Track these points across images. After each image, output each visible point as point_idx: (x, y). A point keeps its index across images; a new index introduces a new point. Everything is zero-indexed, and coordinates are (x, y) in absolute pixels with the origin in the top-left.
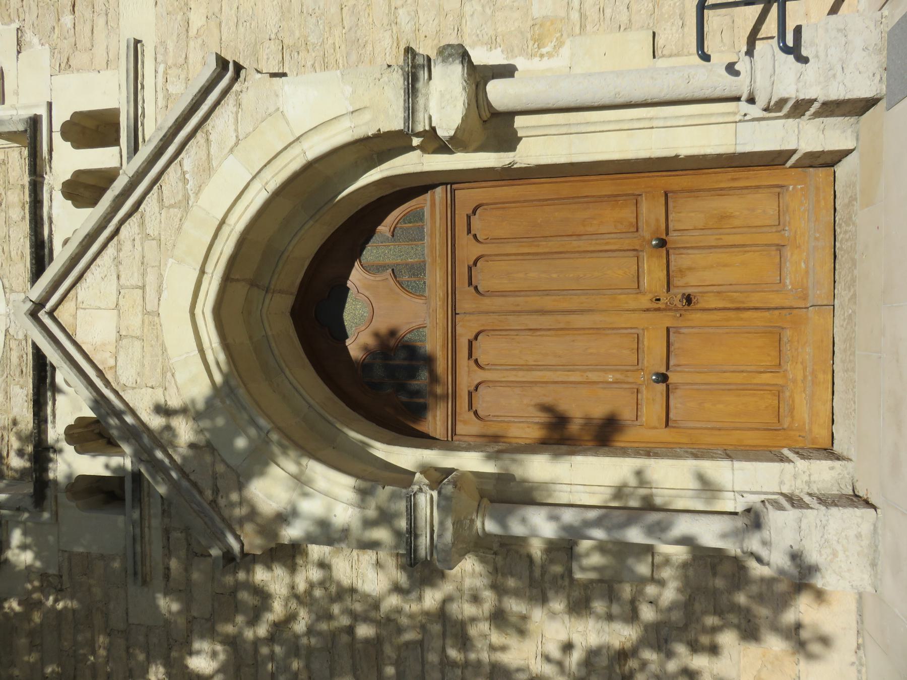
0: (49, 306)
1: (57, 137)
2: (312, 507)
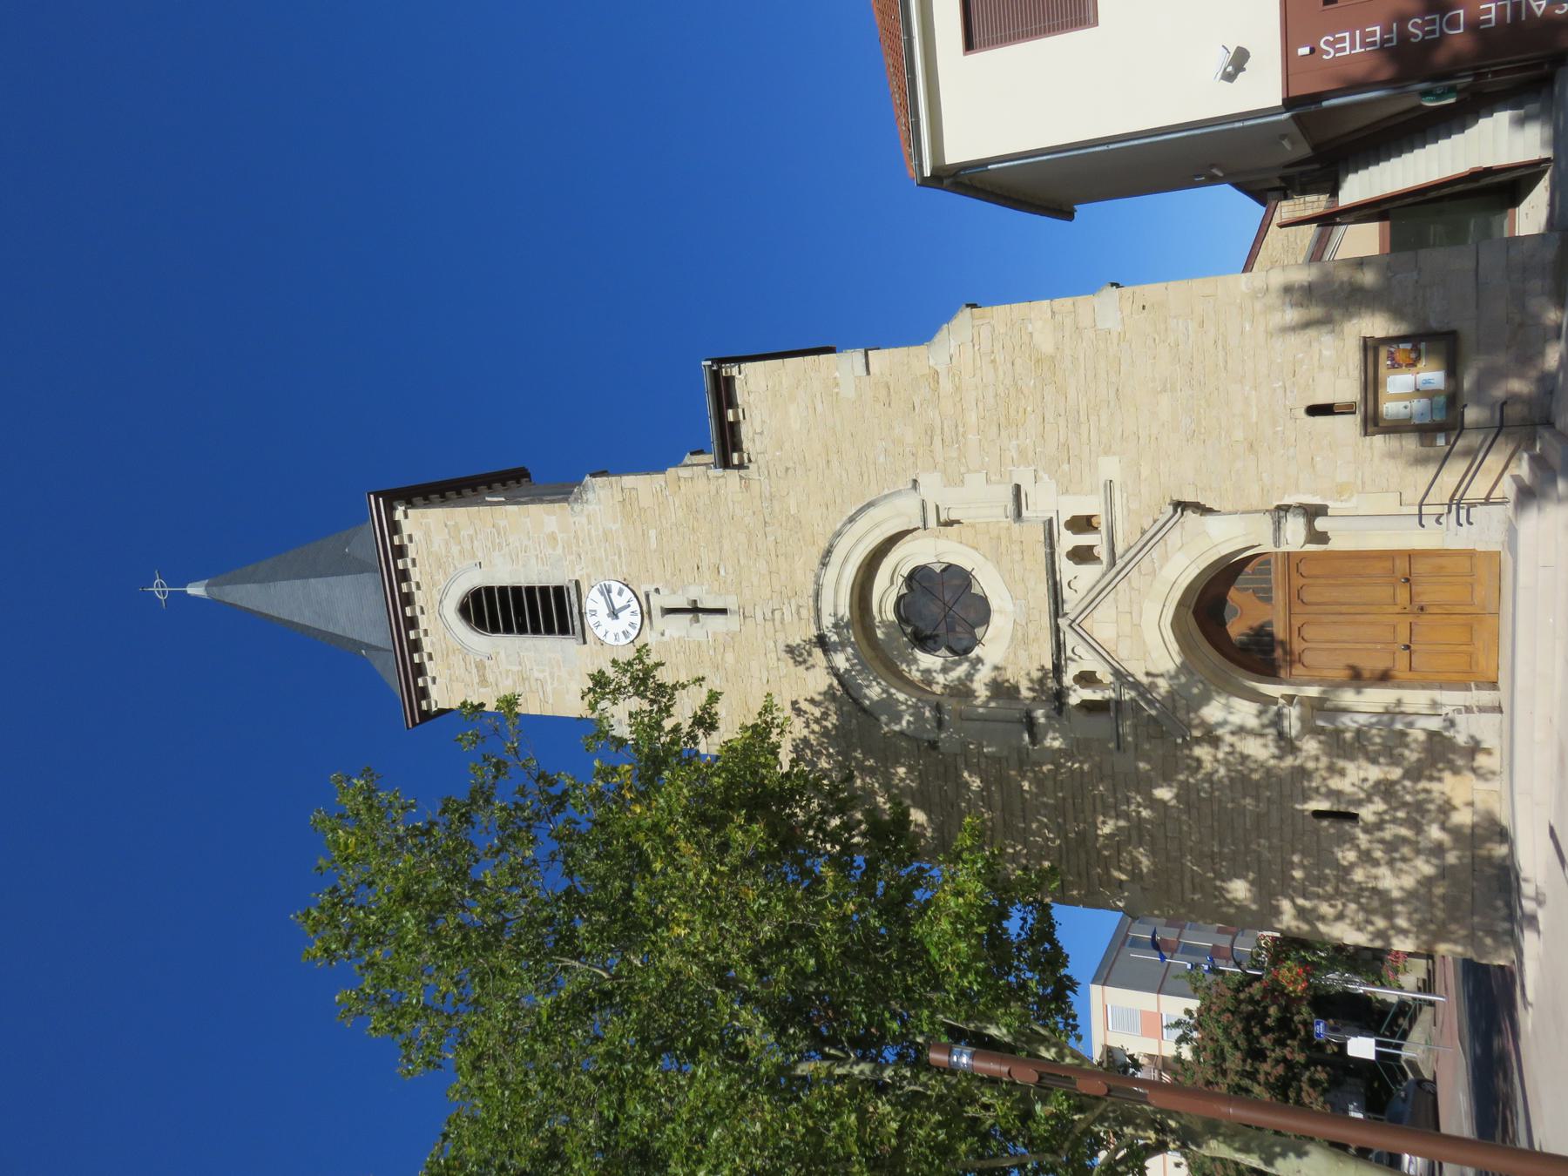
0: (1077, 621)
1: (1062, 528)
2: (1236, 719)
